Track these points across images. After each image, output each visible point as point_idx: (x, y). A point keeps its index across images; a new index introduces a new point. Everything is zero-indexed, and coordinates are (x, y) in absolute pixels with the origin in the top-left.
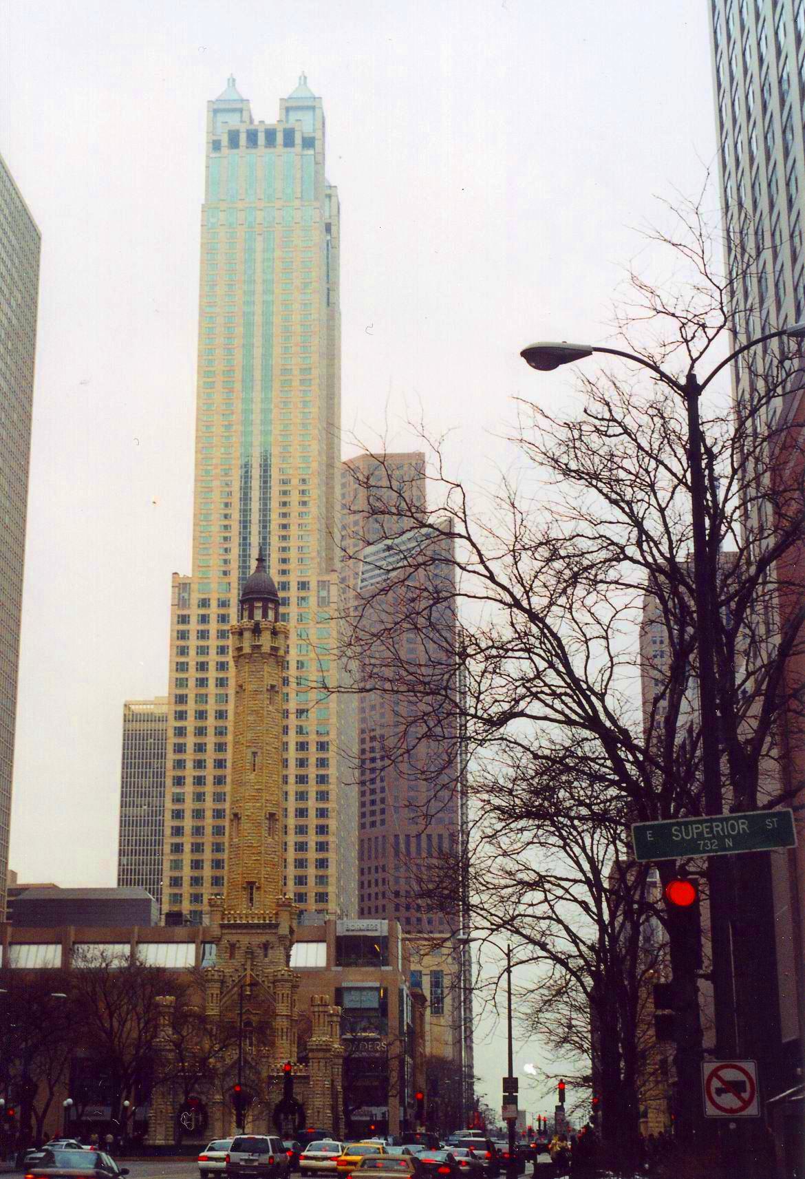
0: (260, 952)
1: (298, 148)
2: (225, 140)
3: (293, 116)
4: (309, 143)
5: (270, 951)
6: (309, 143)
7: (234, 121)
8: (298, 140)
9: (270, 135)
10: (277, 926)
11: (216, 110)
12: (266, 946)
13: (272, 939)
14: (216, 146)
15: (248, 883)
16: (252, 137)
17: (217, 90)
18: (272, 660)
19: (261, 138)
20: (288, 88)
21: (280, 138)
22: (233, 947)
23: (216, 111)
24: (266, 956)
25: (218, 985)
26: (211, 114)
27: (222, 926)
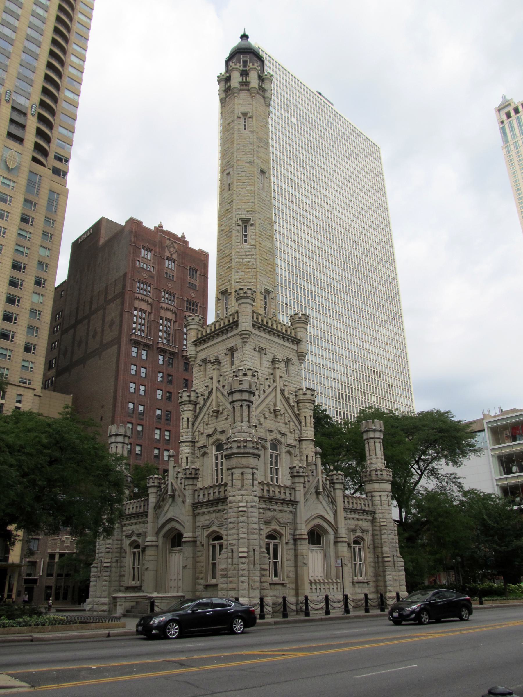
0: (225, 360)
2: (504, 117)
7: (506, 110)
10: (236, 324)
12: (232, 351)
13: (235, 342)
17: (498, 103)
18: (244, 95)
22: (205, 361)
23: (499, 111)
24: (232, 363)
25: (191, 407)
26: (497, 112)
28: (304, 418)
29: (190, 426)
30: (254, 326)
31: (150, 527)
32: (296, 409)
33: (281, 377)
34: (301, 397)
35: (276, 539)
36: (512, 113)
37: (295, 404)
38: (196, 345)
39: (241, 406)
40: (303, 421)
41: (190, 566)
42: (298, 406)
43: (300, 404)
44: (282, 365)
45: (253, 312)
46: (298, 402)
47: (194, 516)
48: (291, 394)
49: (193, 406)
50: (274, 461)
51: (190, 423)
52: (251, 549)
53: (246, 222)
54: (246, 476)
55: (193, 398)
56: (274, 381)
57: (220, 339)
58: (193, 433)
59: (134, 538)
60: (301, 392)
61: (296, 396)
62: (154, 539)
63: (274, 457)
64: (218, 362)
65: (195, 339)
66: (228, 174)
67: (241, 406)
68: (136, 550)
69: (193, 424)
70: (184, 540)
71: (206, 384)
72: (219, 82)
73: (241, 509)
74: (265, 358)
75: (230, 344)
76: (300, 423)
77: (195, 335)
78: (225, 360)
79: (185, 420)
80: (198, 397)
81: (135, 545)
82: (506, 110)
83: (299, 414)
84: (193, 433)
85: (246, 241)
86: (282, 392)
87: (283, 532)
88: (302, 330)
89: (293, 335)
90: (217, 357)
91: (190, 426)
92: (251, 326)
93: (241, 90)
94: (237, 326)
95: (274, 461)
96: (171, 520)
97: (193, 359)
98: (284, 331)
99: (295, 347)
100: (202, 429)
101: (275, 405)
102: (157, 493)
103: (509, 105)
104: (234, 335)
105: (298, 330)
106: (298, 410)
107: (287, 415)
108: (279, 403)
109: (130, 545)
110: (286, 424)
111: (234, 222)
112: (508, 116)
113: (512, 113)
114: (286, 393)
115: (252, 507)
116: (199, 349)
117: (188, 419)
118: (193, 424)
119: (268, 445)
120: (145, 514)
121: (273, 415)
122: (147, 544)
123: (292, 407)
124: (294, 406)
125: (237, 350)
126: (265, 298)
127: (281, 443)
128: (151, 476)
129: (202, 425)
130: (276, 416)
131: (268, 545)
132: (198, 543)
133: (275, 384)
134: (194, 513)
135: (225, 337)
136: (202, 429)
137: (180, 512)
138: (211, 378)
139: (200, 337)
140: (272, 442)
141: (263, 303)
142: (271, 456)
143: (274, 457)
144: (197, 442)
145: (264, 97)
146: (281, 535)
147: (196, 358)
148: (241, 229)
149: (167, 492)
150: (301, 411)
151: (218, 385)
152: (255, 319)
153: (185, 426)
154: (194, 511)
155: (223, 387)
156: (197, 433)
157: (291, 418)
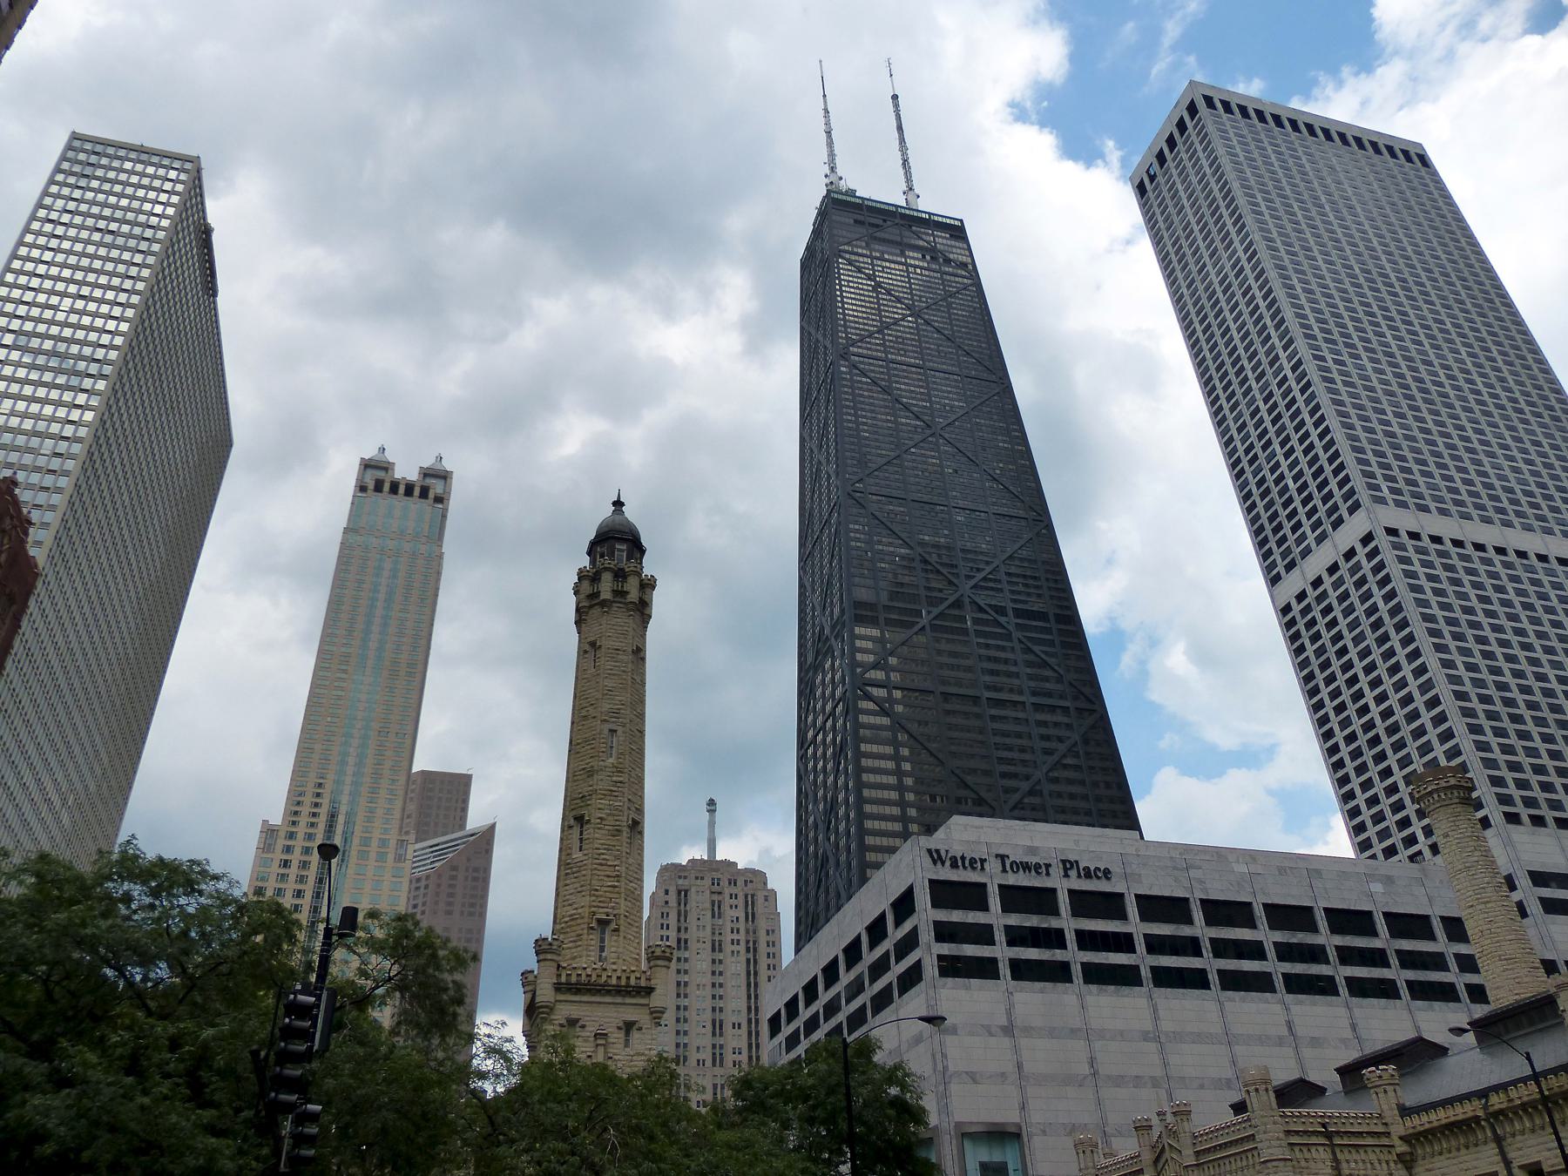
0: (617, 1037)
1: (430, 501)
2: (371, 486)
3: (429, 481)
4: (439, 500)
5: (635, 1035)
6: (439, 500)
7: (381, 474)
8: (431, 495)
9: (409, 490)
10: (649, 991)
11: (367, 465)
12: (629, 1027)
13: (642, 1017)
14: (362, 488)
15: (600, 921)
16: (394, 488)
17: (370, 453)
19: (402, 489)
20: (428, 462)
21: (417, 491)
24: (627, 1044)
27: (558, 988)
36: (387, 487)
57: (608, 999)
66: (613, 731)
75: (630, 1015)
82: (381, 474)
103: (386, 469)
112: (378, 487)
113: (387, 487)
125: (640, 1029)
135: (619, 1000)
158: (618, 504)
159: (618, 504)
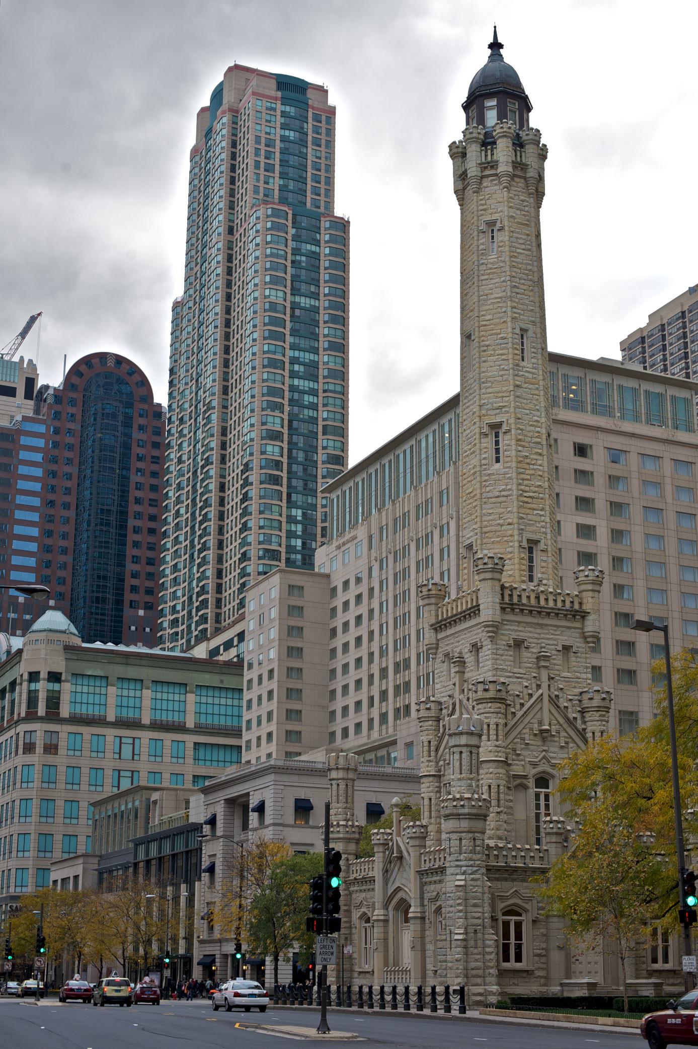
10: (475, 611)
12: (476, 648)
28: (591, 734)
29: (433, 754)
30: (503, 609)
31: (378, 896)
32: (579, 722)
33: (551, 678)
34: (586, 703)
35: (520, 915)
37: (578, 715)
38: (435, 629)
39: (461, 752)
40: (590, 740)
41: (418, 948)
42: (583, 717)
43: (587, 715)
44: (558, 660)
45: (503, 587)
46: (582, 712)
47: (422, 885)
48: (570, 700)
49: (435, 723)
50: (542, 802)
51: (432, 748)
52: (471, 929)
53: (496, 427)
54: (464, 841)
55: (433, 713)
56: (539, 686)
58: (437, 763)
59: (364, 909)
60: (585, 697)
61: (580, 701)
62: (382, 912)
63: (542, 797)
64: (462, 663)
65: (433, 621)
67: (461, 752)
68: (367, 925)
69: (437, 750)
70: (410, 915)
71: (450, 693)
72: (452, 156)
73: (457, 883)
74: (525, 654)
76: (586, 741)
77: (433, 613)
78: (469, 659)
79: (426, 744)
80: (441, 710)
81: (365, 918)
83: (584, 730)
84: (437, 763)
85: (498, 460)
86: (554, 701)
87: (527, 906)
88: (590, 594)
89: (576, 607)
90: (460, 653)
91: (433, 754)
92: (498, 612)
93: (482, 177)
94: (479, 610)
95: (542, 802)
96: (398, 889)
97: (434, 651)
98: (559, 604)
99: (578, 625)
100: (447, 758)
101: (540, 723)
102: (384, 852)
104: (477, 624)
105: (584, 594)
106: (584, 722)
107: (563, 734)
108: (546, 721)
109: (361, 918)
110: (562, 747)
111: (477, 430)
114: (563, 703)
115: (473, 880)
116: (440, 636)
117: (430, 742)
118: (437, 750)
119: (531, 783)
120: (372, 880)
121: (539, 738)
122: (375, 918)
123: (571, 722)
124: (575, 718)
125: (482, 647)
126: (531, 550)
127: (553, 777)
128: (376, 831)
129: (447, 750)
130: (544, 740)
131: (506, 925)
132: (427, 921)
133: (540, 691)
134: (421, 882)
136: (447, 758)
137: (407, 882)
138: (454, 684)
139: (440, 618)
140: (536, 777)
141: (526, 562)
142: (537, 796)
143: (542, 797)
144: (444, 775)
145: (525, 178)
146: (526, 911)
147: (437, 648)
148: (488, 443)
149: (393, 853)
150: (588, 724)
151: (461, 697)
152: (507, 599)
153: (425, 754)
154: (421, 879)
155: (468, 699)
156: (441, 763)
157: (571, 738)
158: (496, 46)
159: (496, 46)
